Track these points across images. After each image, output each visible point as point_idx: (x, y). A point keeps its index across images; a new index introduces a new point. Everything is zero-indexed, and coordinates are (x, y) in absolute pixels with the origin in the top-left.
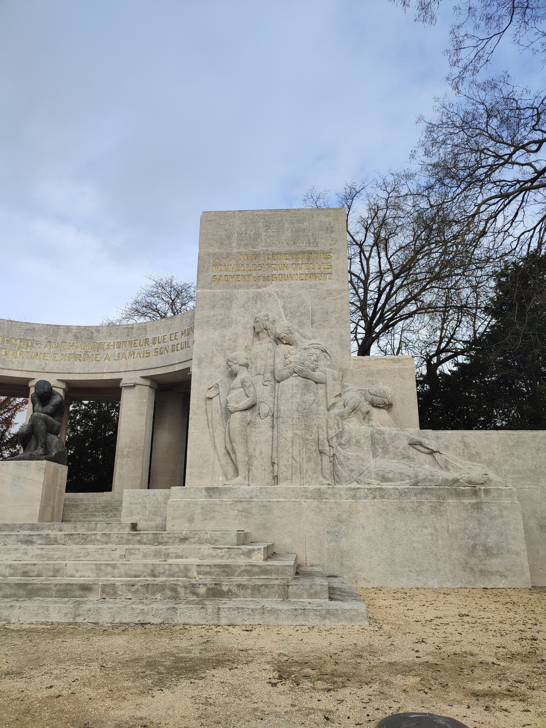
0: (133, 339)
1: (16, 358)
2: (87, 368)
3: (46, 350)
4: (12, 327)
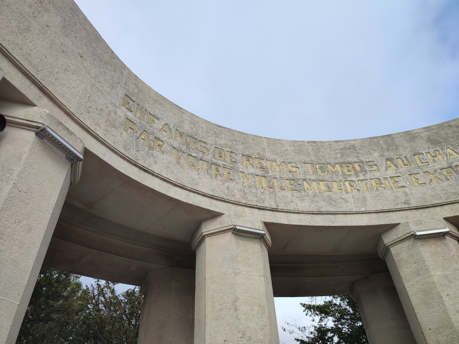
1: (347, 193)
3: (391, 172)
4: (319, 149)
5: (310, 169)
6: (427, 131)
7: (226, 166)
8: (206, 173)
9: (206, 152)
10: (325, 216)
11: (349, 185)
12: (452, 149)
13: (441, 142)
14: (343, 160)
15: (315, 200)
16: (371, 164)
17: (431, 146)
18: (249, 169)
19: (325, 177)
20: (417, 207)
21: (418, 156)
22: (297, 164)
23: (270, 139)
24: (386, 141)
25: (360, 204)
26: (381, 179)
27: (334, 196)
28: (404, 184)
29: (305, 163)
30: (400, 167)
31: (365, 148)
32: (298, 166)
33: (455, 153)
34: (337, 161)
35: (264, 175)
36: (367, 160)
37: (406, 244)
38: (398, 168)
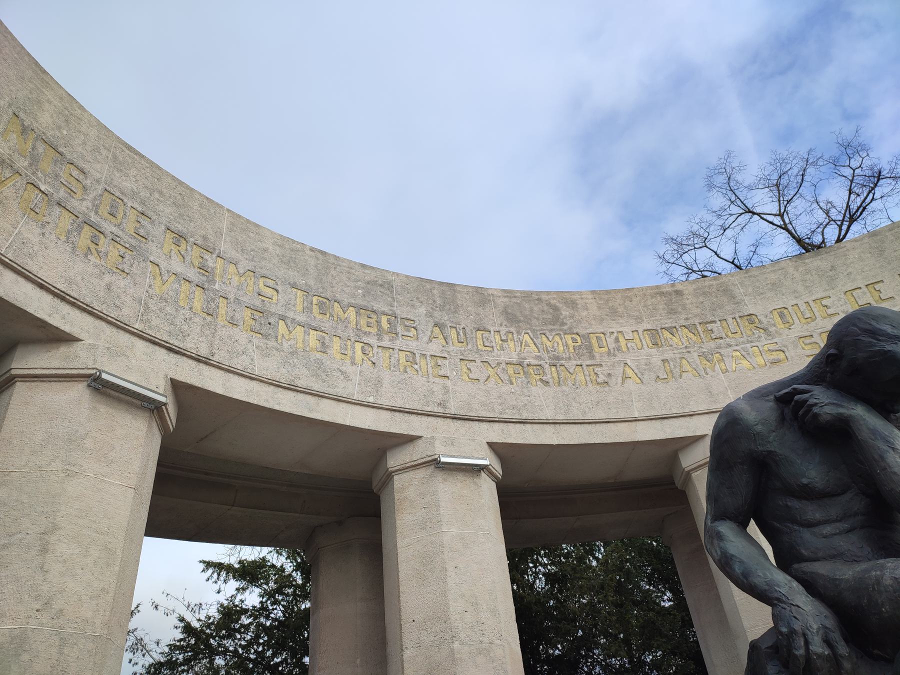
0: (697, 321)
1: (353, 363)
2: (574, 404)
3: (435, 348)
5: (299, 301)
6: (507, 296)
7: (118, 239)
8: (63, 238)
9: (79, 192)
10: (301, 396)
11: (360, 350)
12: (532, 336)
13: (520, 321)
14: (365, 303)
15: (291, 361)
16: (410, 324)
17: (505, 323)
18: (172, 262)
19: (323, 325)
20: (455, 416)
21: (483, 332)
22: (277, 284)
23: (239, 216)
24: (443, 293)
25: (368, 389)
26: (417, 355)
27: (328, 362)
28: (448, 372)
29: (294, 286)
30: (451, 343)
31: (408, 293)
32: (279, 288)
33: (533, 345)
34: (354, 302)
35: (203, 284)
36: (404, 316)
37: (421, 473)
38: (447, 343)
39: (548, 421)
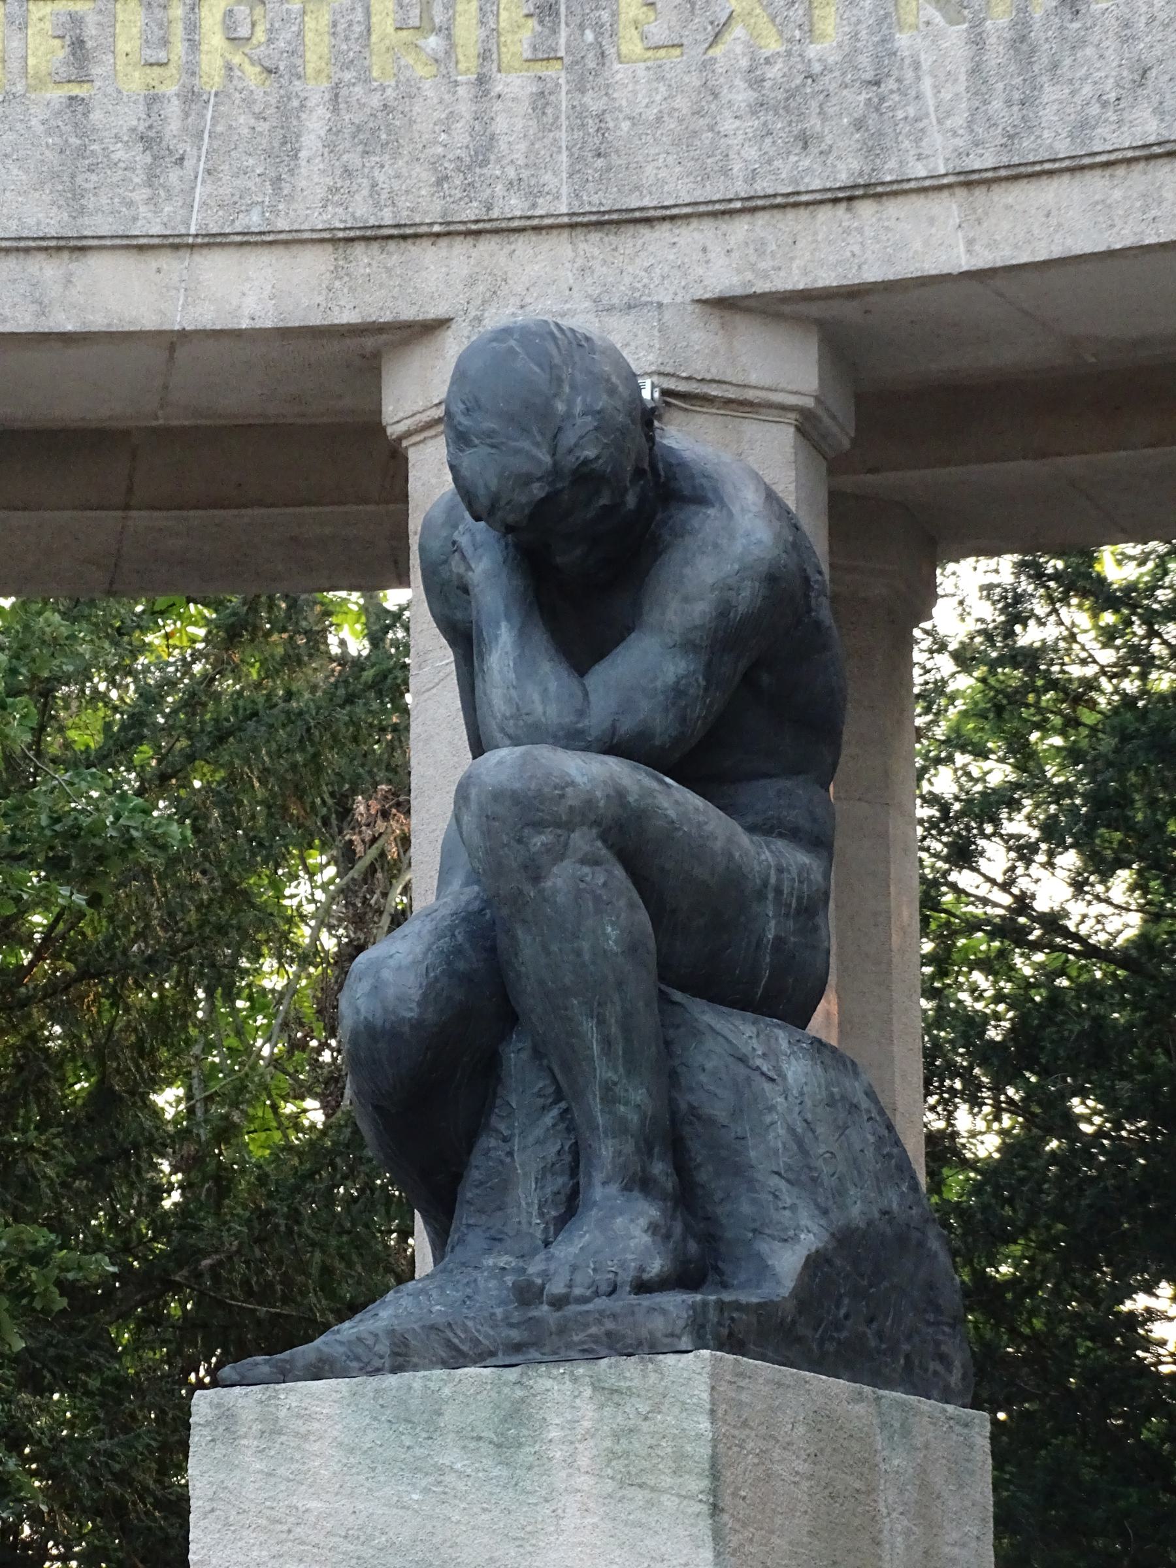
11: (218, 28)
39: (935, 182)
